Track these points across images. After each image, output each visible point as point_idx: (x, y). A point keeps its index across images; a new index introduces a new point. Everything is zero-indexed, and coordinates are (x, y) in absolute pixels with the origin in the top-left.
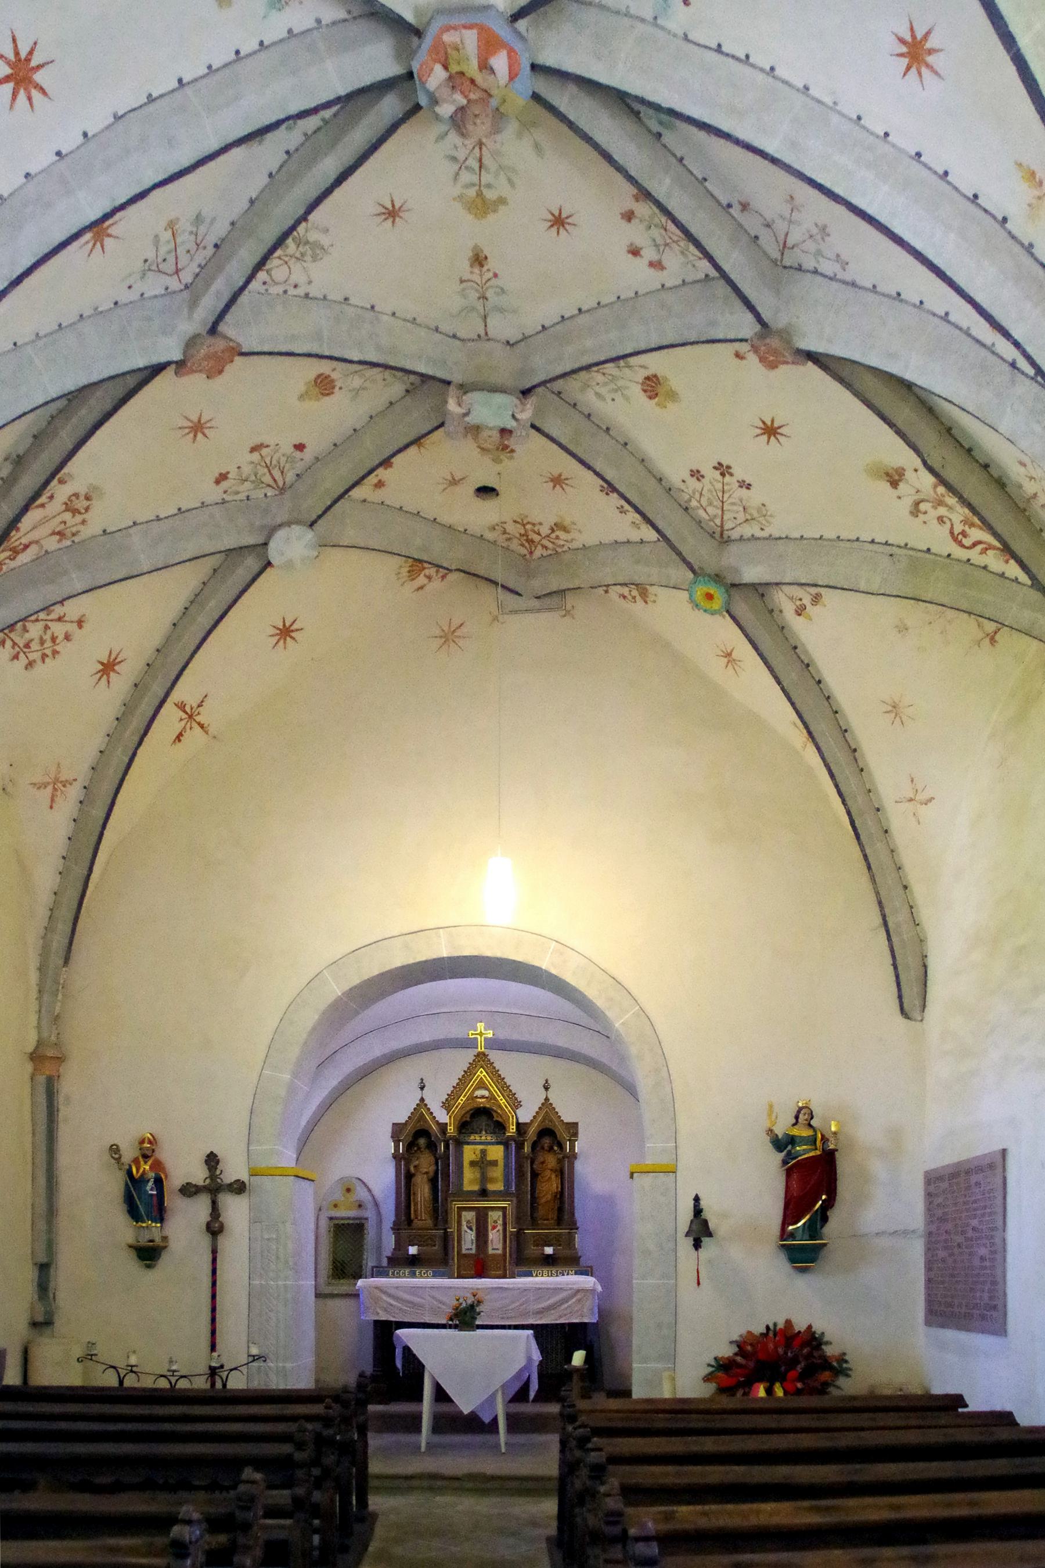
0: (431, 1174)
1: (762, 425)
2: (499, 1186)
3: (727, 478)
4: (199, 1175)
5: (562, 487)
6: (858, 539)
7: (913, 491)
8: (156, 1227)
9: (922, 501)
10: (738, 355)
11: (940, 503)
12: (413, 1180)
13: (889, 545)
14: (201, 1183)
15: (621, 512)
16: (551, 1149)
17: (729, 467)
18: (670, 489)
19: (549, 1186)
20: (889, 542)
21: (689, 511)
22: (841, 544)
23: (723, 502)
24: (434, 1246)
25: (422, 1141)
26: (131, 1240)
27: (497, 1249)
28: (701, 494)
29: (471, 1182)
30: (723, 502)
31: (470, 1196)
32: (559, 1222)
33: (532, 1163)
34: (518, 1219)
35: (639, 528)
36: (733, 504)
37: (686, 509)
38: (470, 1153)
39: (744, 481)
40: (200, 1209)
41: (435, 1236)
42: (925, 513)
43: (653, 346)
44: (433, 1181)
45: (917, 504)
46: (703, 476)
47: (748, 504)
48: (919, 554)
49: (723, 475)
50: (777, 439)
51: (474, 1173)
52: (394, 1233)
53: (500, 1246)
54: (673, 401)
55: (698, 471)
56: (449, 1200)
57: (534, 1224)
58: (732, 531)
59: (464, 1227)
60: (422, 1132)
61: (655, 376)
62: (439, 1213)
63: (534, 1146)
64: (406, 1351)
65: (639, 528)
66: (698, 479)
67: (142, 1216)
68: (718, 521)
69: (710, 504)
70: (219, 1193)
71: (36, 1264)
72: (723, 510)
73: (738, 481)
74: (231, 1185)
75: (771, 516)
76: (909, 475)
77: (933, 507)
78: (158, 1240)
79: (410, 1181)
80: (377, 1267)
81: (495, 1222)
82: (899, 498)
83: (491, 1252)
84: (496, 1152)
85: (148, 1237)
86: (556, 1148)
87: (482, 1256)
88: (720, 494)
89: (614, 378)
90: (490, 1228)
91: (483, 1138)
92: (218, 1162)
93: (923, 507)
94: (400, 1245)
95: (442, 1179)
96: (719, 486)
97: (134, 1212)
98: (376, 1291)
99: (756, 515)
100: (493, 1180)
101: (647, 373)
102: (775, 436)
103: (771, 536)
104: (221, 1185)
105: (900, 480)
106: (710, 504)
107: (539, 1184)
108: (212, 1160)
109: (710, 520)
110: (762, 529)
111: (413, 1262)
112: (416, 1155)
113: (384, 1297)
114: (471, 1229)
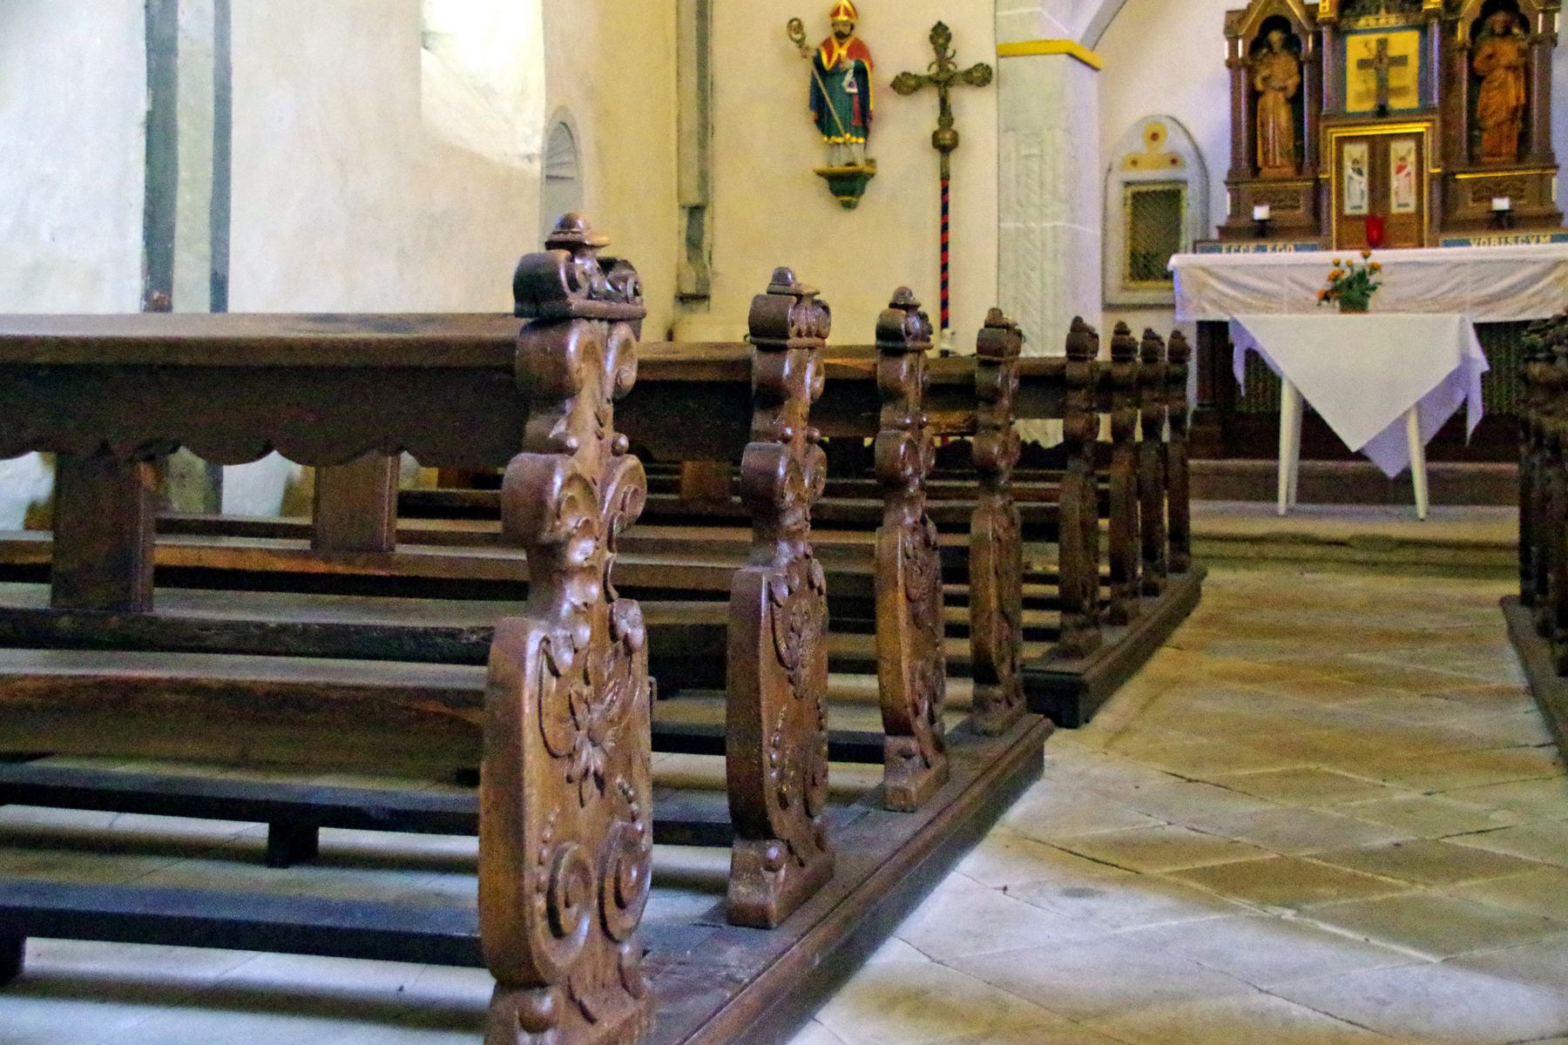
0: (1291, 91)
2: (1411, 101)
4: (921, 61)
8: (857, 143)
12: (1261, 102)
14: (924, 72)
16: (1507, 32)
19: (1503, 94)
24: (1298, 207)
25: (1276, 37)
26: (821, 165)
27: (1406, 205)
29: (1360, 97)
31: (1359, 119)
32: (1521, 155)
33: (1471, 59)
34: (1445, 156)
38: (1357, 47)
40: (922, 113)
41: (1297, 192)
44: (1295, 101)
51: (1365, 81)
52: (1229, 190)
53: (1412, 201)
56: (1322, 125)
57: (1473, 162)
59: (1348, 170)
60: (1278, 22)
62: (1306, 155)
63: (1476, 28)
64: (1253, 358)
67: (838, 129)
70: (951, 86)
71: (684, 207)
74: (969, 72)
78: (861, 165)
79: (1256, 105)
80: (1201, 241)
81: (1403, 159)
83: (1394, 210)
84: (1406, 43)
85: (845, 159)
86: (1516, 30)
87: (1379, 215)
90: (1393, 171)
91: (1382, 21)
92: (948, 38)
94: (1239, 207)
95: (1310, 95)
97: (824, 123)
98: (1200, 273)
100: (1401, 92)
104: (956, 74)
107: (1483, 94)
108: (940, 35)
111: (1262, 232)
112: (1265, 60)
113: (1213, 282)
114: (1360, 173)
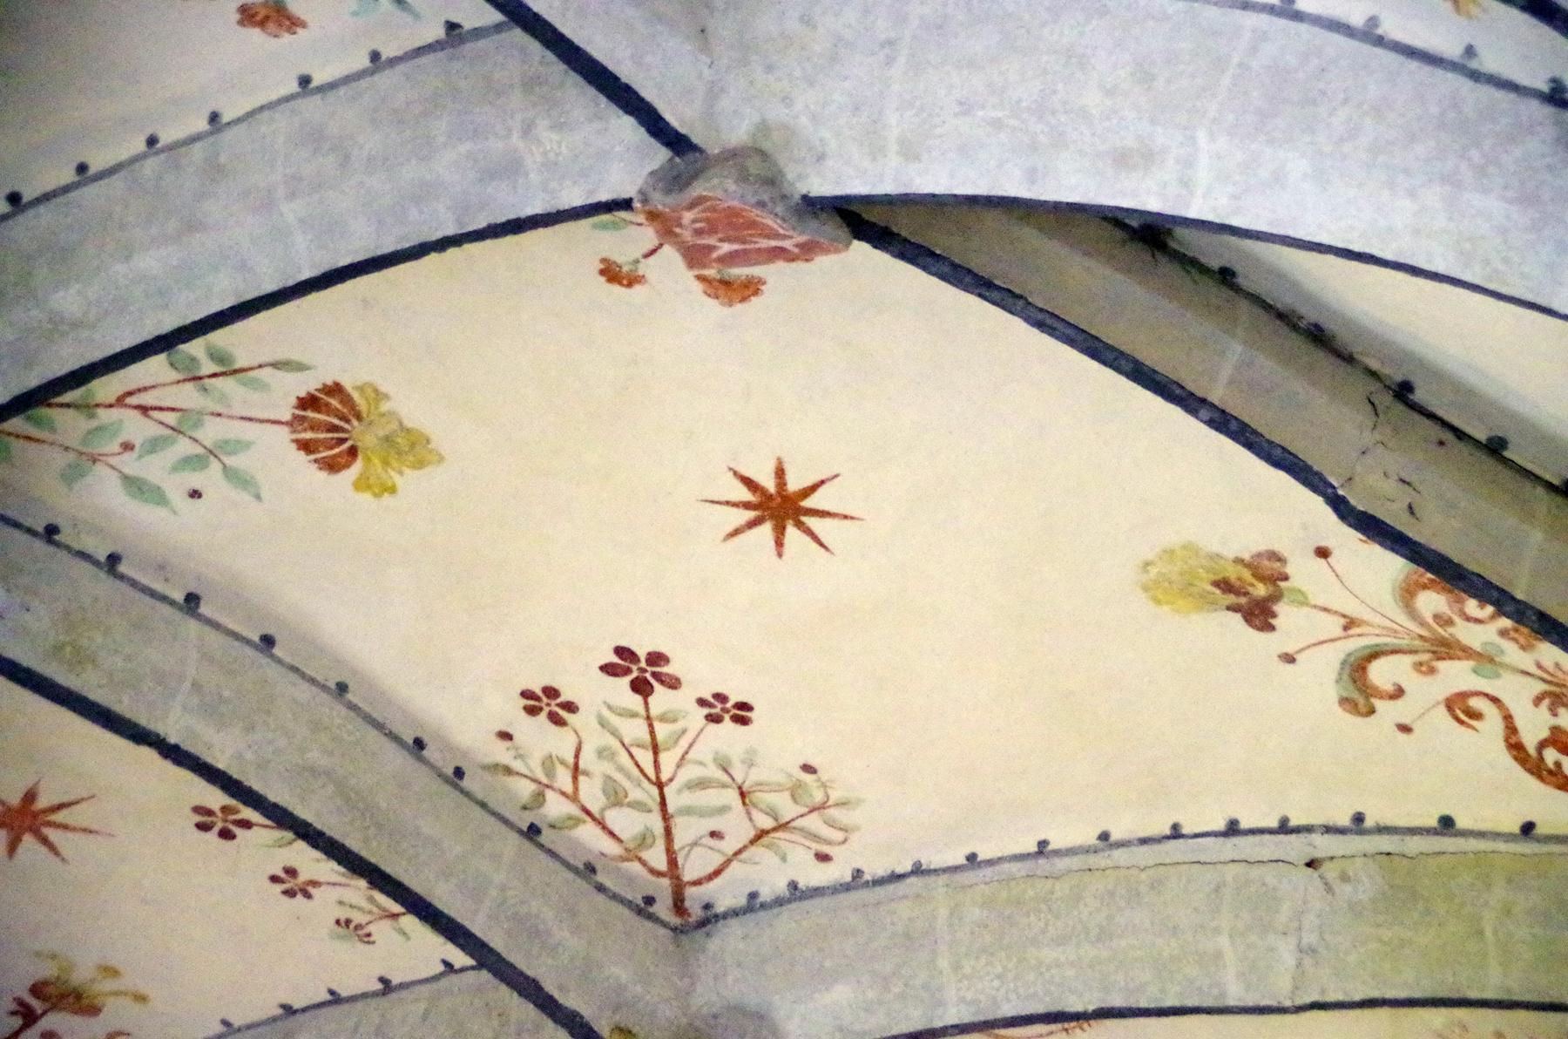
1: (745, 495)
3: (661, 698)
5: (45, 841)
6: (1176, 833)
7: (1334, 626)
9: (1375, 654)
10: (611, 273)
11: (1446, 649)
13: (1297, 830)
15: (290, 893)
17: (656, 658)
18: (459, 773)
20: (1293, 822)
21: (546, 837)
22: (1120, 855)
23: (660, 786)
28: (576, 771)
30: (660, 786)
35: (367, 938)
36: (701, 784)
37: (533, 832)
39: (720, 697)
42: (1399, 693)
43: (306, 274)
45: (1357, 669)
46: (570, 707)
47: (754, 776)
48: (1415, 845)
49: (641, 687)
50: (809, 532)
54: (420, 464)
55: (551, 692)
58: (718, 881)
61: (336, 389)
65: (367, 938)
66: (556, 720)
68: (658, 858)
69: (616, 798)
72: (666, 817)
73: (702, 702)
75: (842, 804)
76: (1303, 572)
77: (1418, 666)
82: (1289, 659)
88: (645, 758)
89: (185, 423)
93: (1381, 673)
96: (635, 730)
99: (788, 810)
101: (308, 384)
102: (799, 525)
103: (858, 873)
105: (1276, 597)
106: (616, 798)
109: (623, 859)
110: (823, 858)
